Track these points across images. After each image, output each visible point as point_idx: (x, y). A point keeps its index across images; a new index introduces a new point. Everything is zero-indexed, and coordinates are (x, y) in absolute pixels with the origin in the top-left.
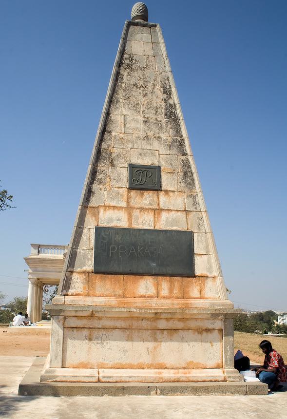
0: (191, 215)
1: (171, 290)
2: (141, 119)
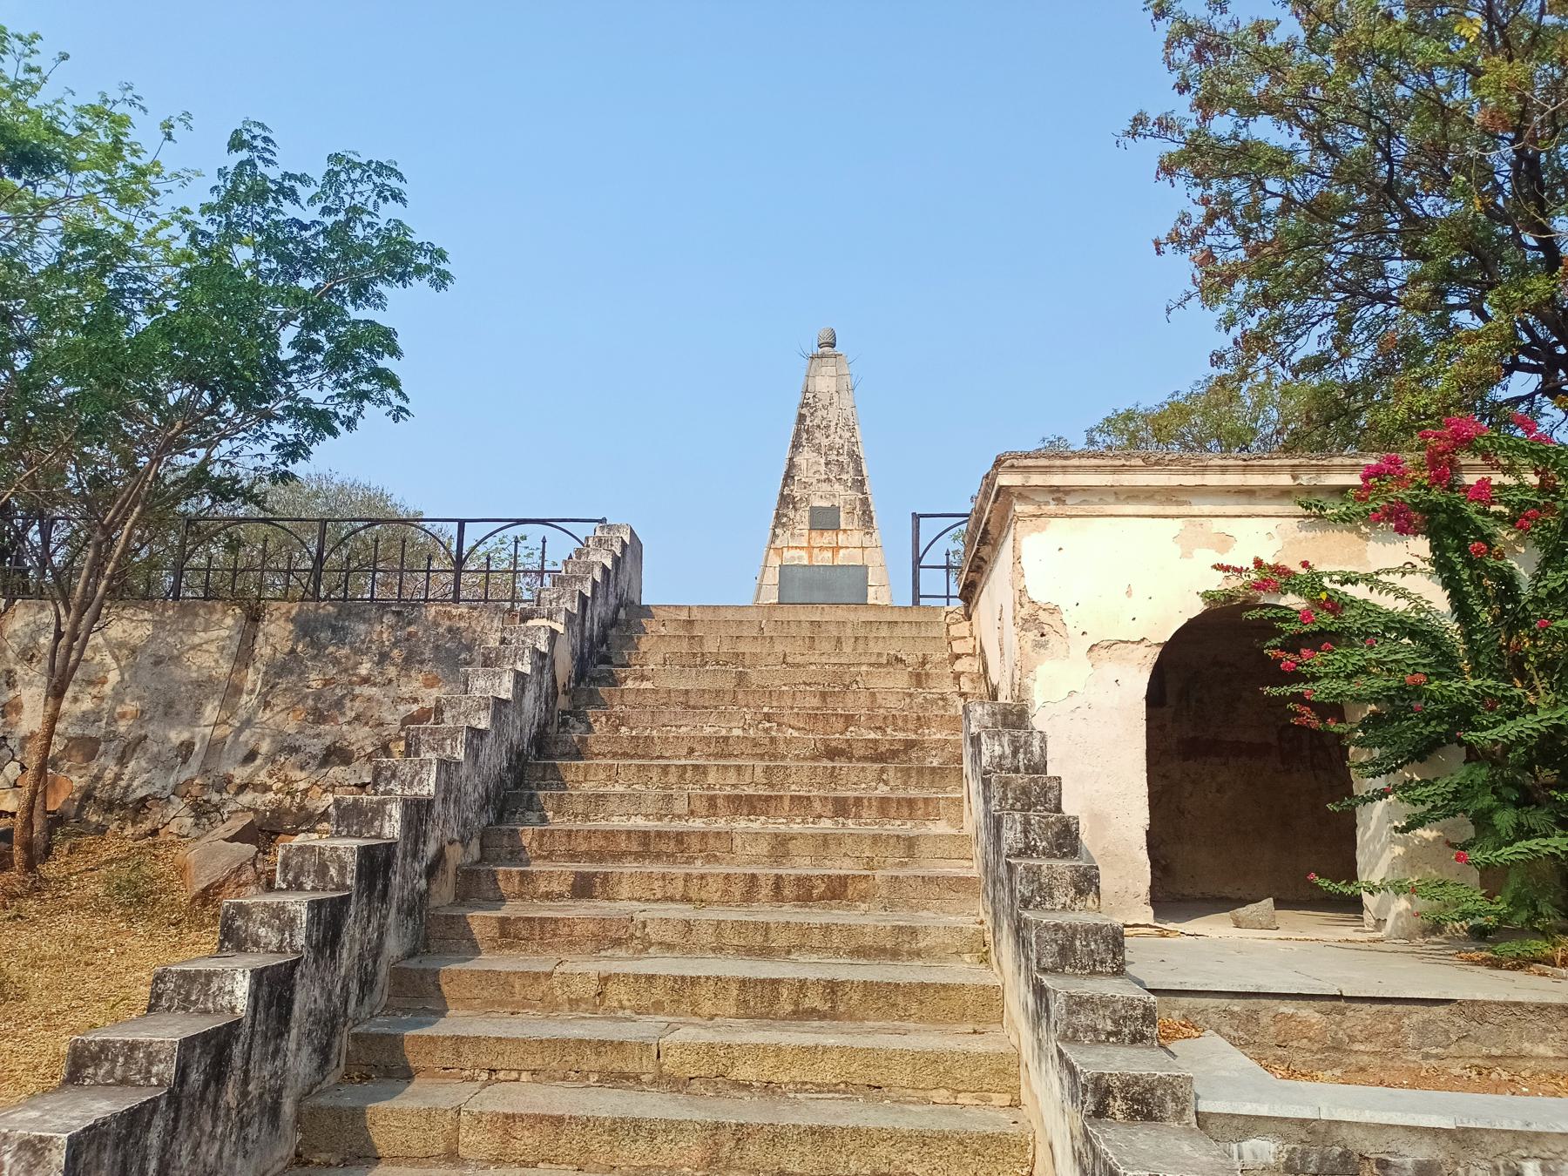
2: (823, 461)
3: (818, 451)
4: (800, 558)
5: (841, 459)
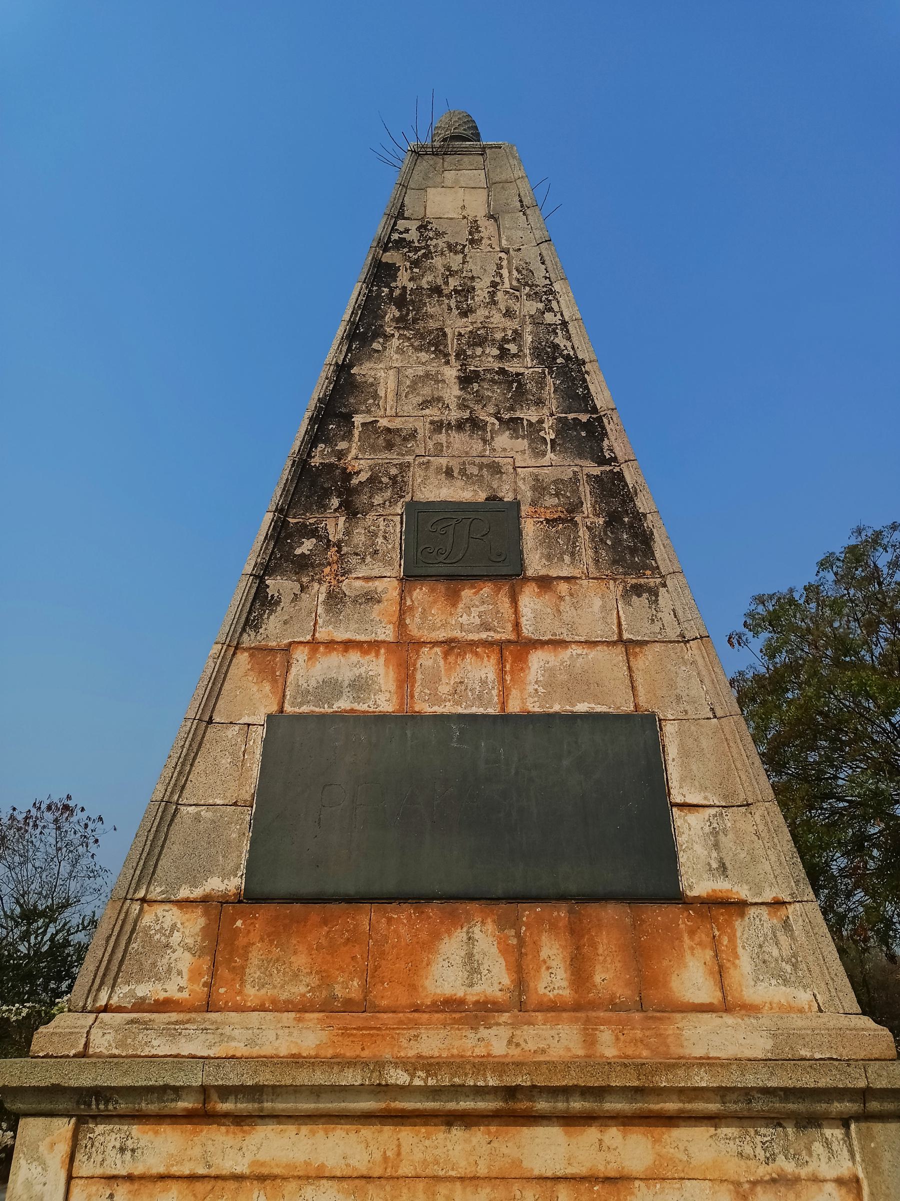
0: (644, 661)
1: (580, 970)
2: (451, 373)
3: (436, 343)
4: (360, 686)
5: (513, 367)
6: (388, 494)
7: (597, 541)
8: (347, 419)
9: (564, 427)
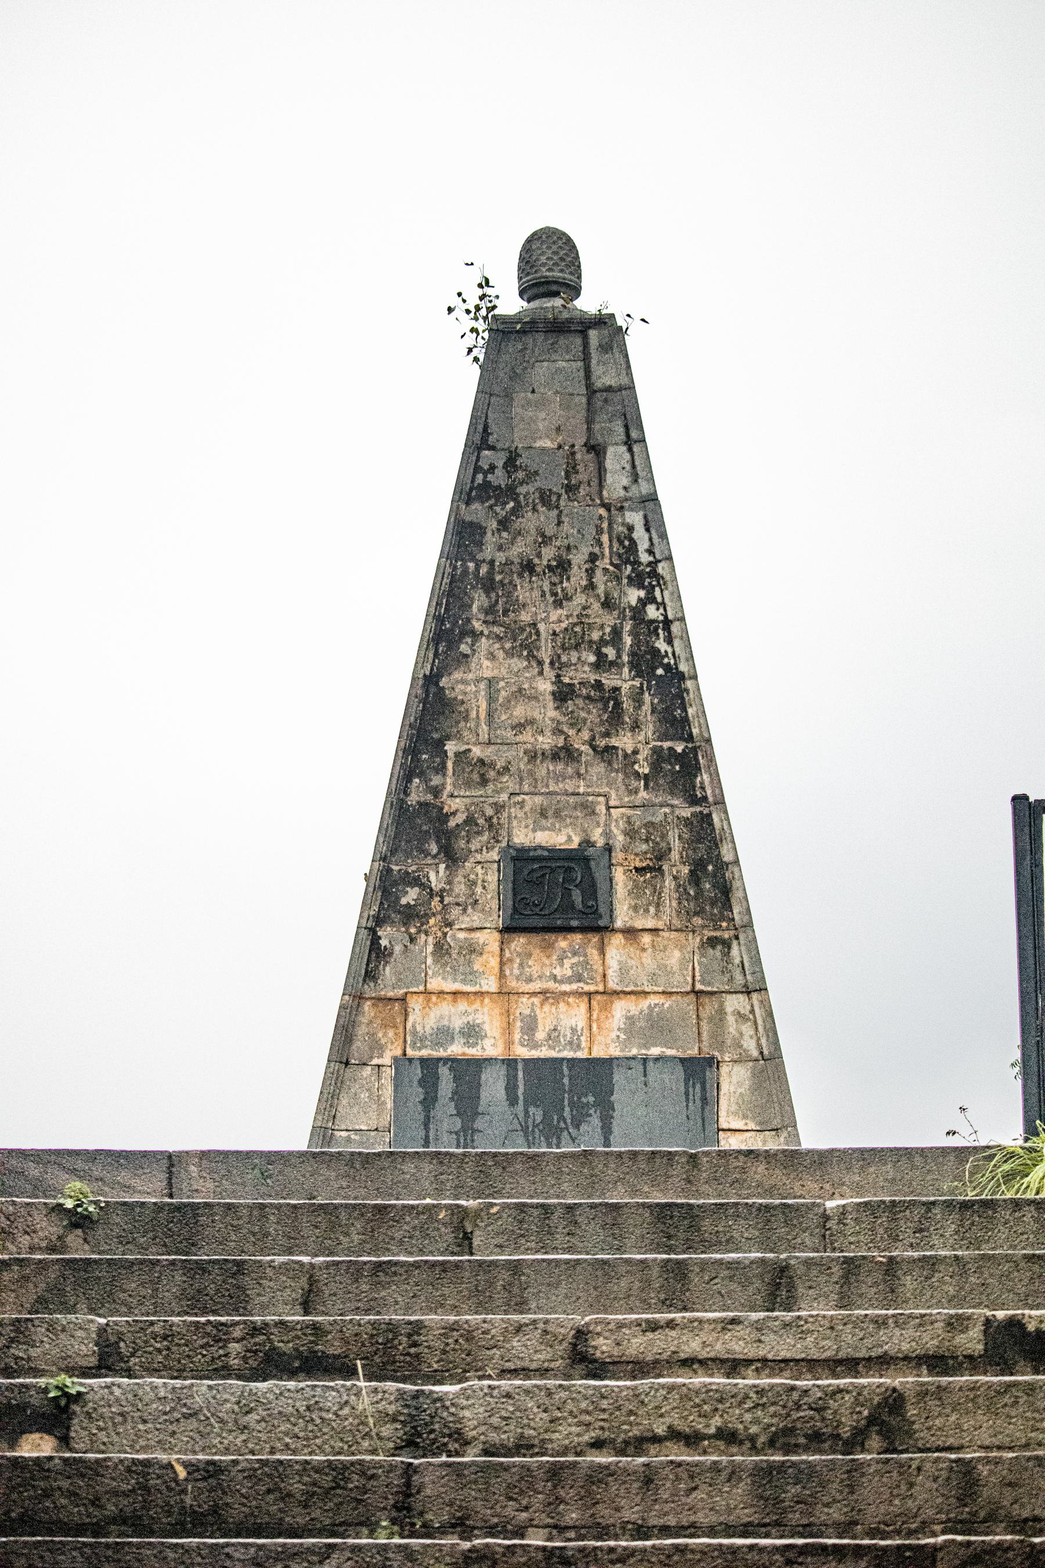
2: (545, 686)
5: (609, 681)
6: (485, 838)
7: (682, 894)
8: (440, 744)
9: (658, 758)
